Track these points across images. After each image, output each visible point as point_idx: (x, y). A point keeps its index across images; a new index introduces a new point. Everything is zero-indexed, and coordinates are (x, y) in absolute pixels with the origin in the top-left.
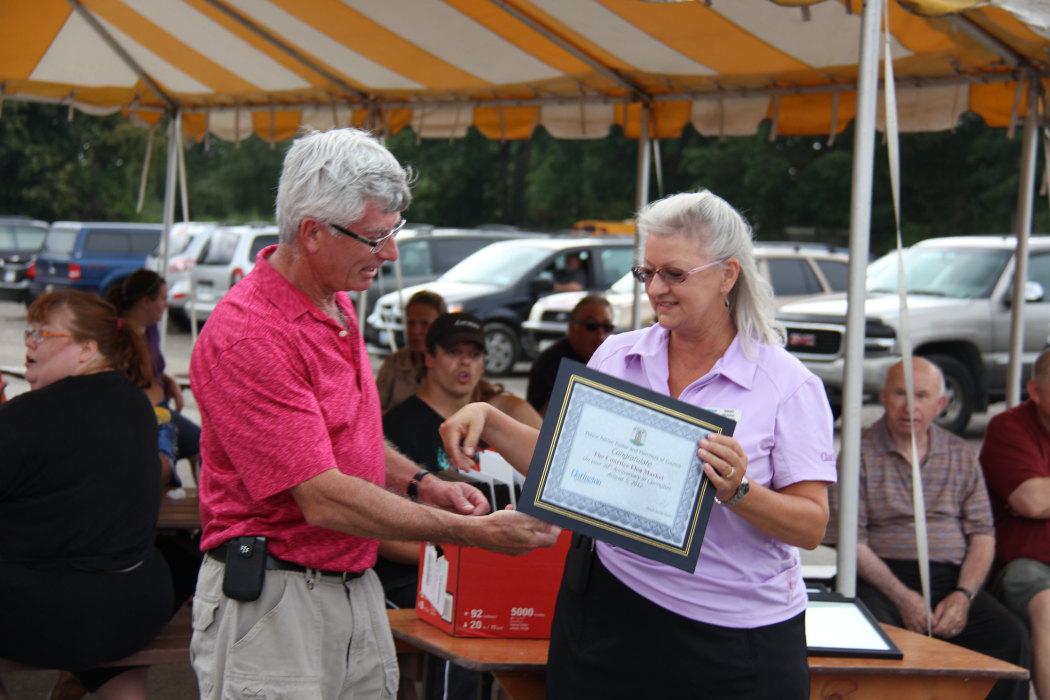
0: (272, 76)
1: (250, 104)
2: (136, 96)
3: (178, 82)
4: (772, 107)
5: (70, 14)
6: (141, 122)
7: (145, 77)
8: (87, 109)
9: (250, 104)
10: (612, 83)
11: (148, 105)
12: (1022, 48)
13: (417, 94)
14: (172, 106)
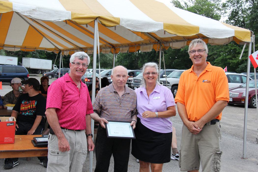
0: (71, 47)
1: (69, 50)
3: (60, 48)
4: (129, 49)
5: (43, 38)
6: (56, 53)
7: (56, 46)
9: (69, 50)
10: (109, 45)
11: (57, 51)
12: (159, 40)
13: (87, 48)
14: (60, 51)
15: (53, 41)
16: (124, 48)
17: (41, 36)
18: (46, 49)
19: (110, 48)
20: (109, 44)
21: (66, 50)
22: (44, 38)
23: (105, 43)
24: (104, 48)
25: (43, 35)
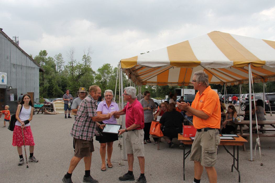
0: (232, 80)
2: (221, 83)
6: (222, 85)
7: (221, 80)
8: (216, 84)
10: (259, 77)
14: (224, 83)
15: (218, 77)
16: (271, 78)
17: (212, 75)
18: (215, 83)
19: (260, 78)
20: (260, 76)
21: (228, 83)
22: (213, 76)
23: (256, 76)
24: (256, 79)
25: (213, 74)
